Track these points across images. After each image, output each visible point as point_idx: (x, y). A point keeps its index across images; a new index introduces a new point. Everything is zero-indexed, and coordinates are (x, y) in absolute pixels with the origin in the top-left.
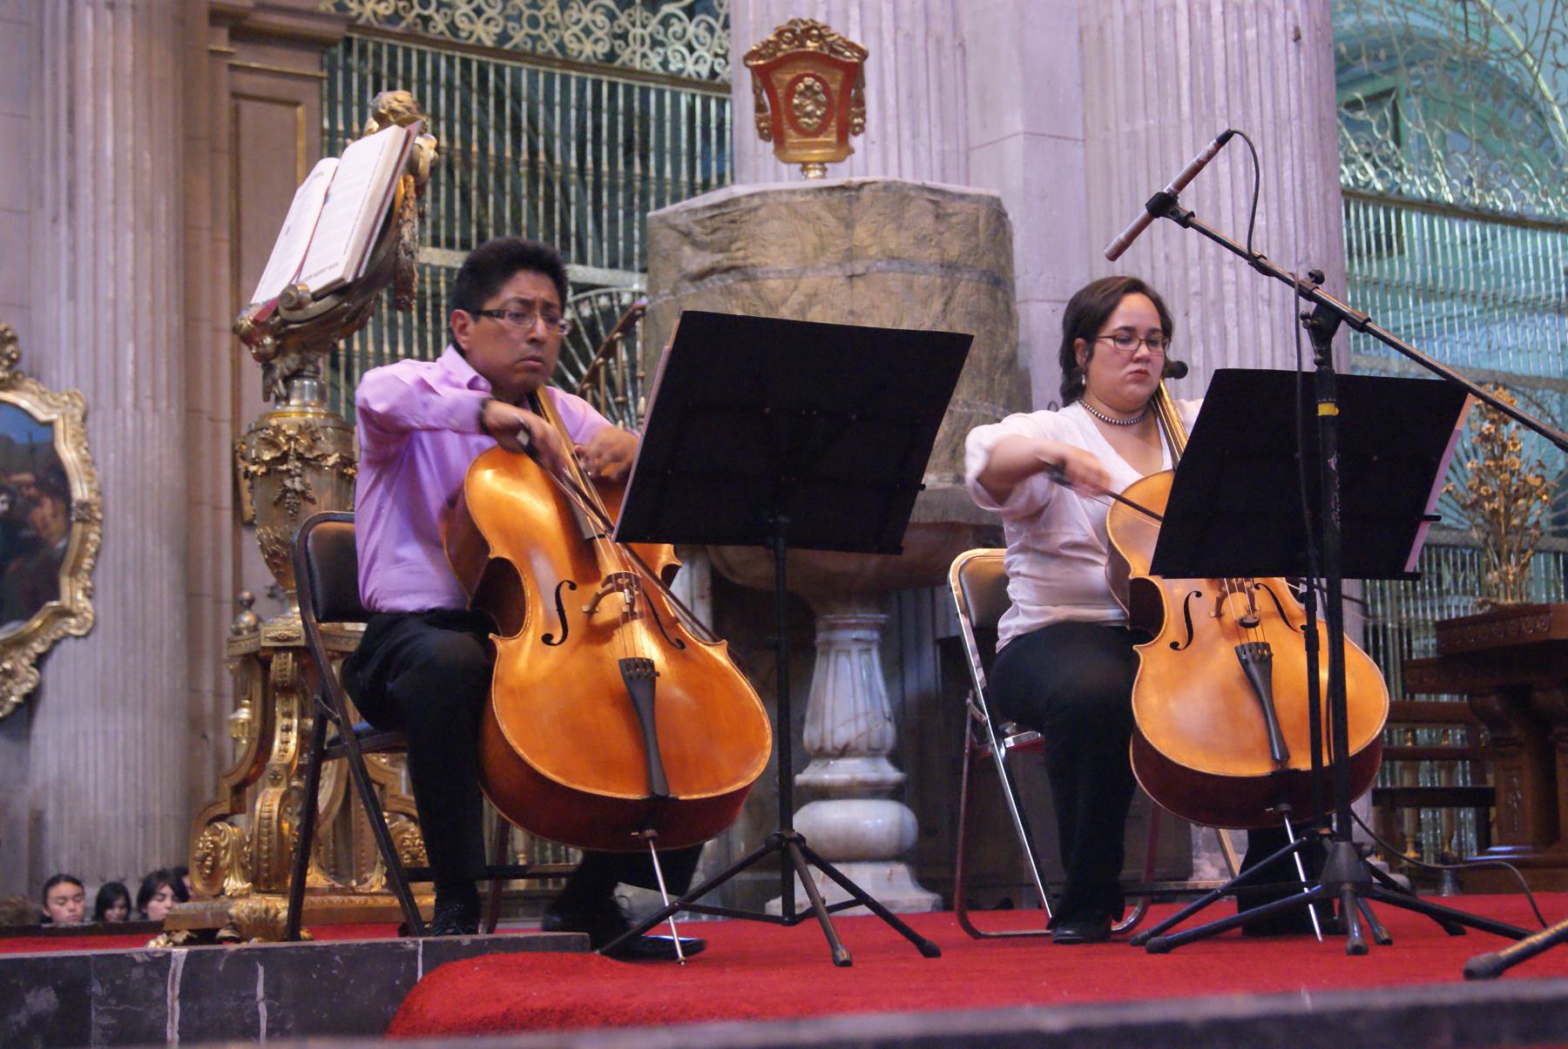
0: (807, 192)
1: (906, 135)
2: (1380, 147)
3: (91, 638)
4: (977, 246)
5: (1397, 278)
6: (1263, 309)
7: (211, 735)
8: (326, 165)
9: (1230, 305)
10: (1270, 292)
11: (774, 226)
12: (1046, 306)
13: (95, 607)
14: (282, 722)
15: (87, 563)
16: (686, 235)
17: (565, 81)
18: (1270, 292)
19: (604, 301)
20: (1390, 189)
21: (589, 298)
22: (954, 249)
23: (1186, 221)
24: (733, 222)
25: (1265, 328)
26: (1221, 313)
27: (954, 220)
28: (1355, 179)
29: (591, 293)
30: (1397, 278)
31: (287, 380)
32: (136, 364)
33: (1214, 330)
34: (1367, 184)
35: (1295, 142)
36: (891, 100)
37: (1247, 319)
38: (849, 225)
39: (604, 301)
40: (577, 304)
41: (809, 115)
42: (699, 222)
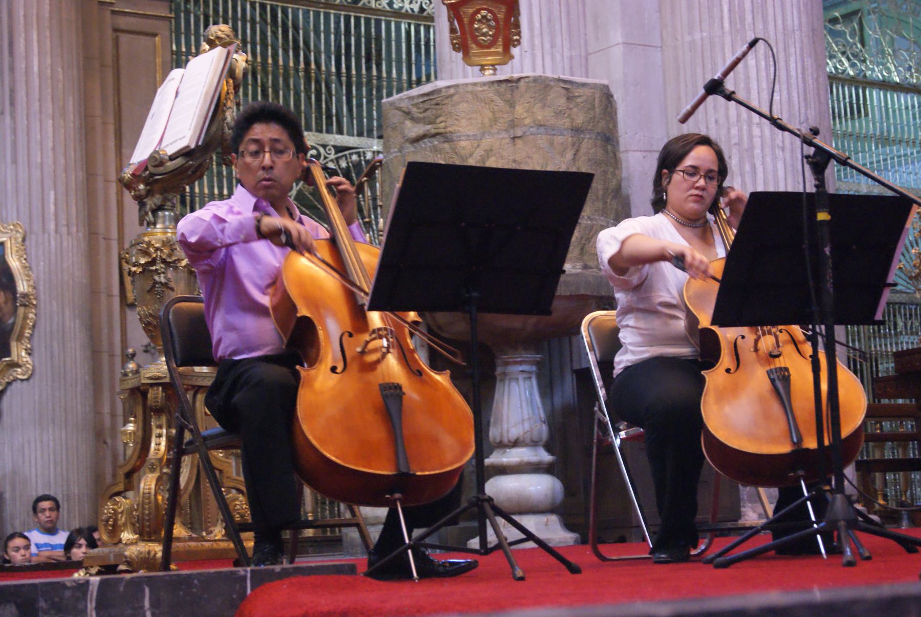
0: (484, 84)
1: (547, 46)
2: (851, 47)
3: (31, 381)
4: (594, 117)
5: (864, 132)
6: (779, 153)
7: (109, 441)
8: (176, 73)
9: (757, 151)
10: (783, 142)
11: (464, 106)
12: (639, 153)
13: (33, 361)
14: (156, 431)
15: (27, 332)
16: (407, 113)
17: (327, 16)
18: (783, 142)
19: (355, 157)
20: (858, 74)
21: (345, 156)
22: (580, 119)
23: (729, 97)
24: (438, 104)
25: (780, 165)
26: (752, 156)
27: (579, 100)
28: (836, 68)
29: (347, 153)
30: (864, 132)
31: (154, 212)
32: (56, 204)
33: (747, 167)
34: (844, 71)
35: (797, 45)
36: (537, 24)
37: (768, 159)
38: (512, 105)
39: (355, 157)
40: (337, 159)
41: (484, 35)
42: (415, 105)
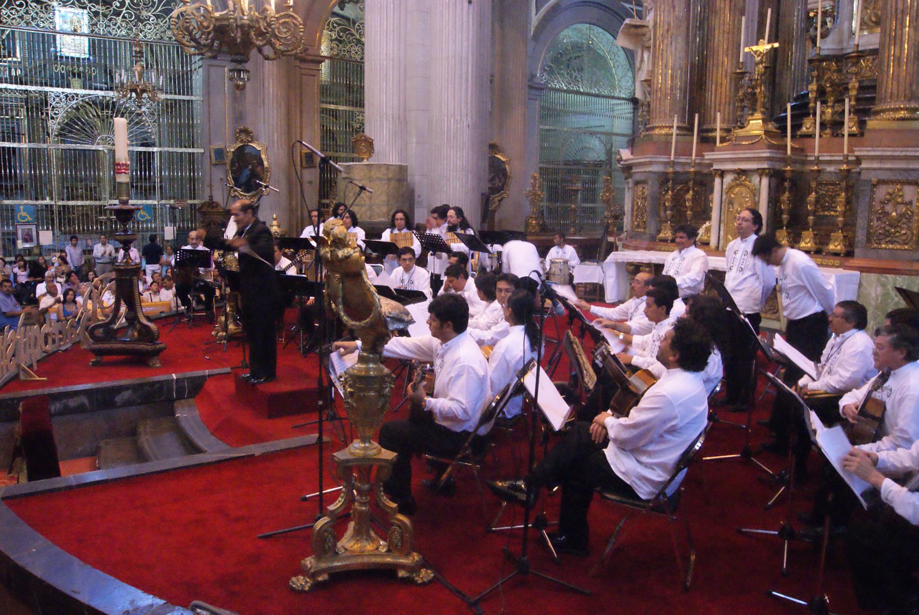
22: (391, 176)
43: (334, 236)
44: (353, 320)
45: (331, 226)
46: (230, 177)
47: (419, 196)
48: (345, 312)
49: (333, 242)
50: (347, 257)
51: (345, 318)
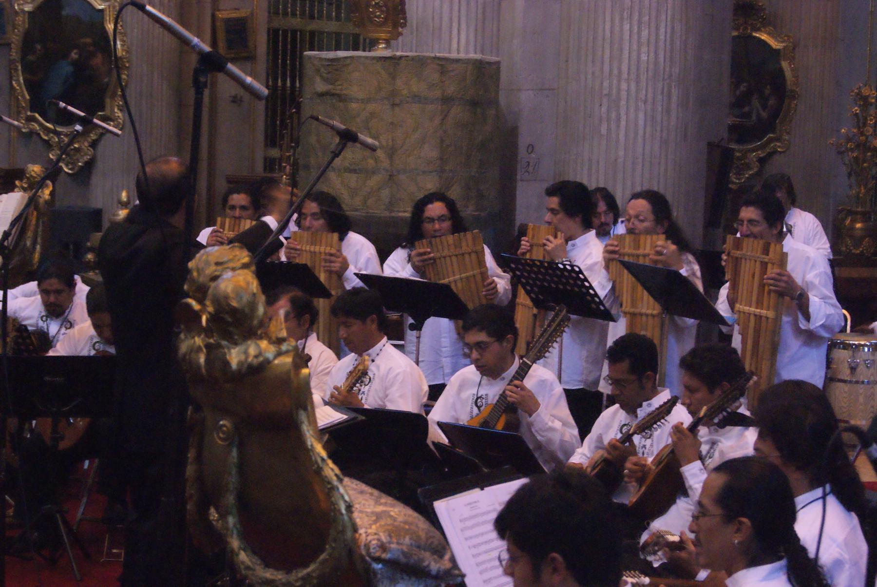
0: (373, 58)
6: (641, 105)
9: (623, 103)
11: (356, 74)
12: (531, 92)
24: (337, 70)
25: (641, 116)
26: (619, 107)
27: (452, 74)
35: (669, 13)
37: (632, 111)
38: (394, 78)
41: (379, 17)
42: (323, 65)
43: (216, 301)
44: (267, 565)
45: (210, 270)
46: (19, 82)
47: (531, 148)
48: (246, 536)
49: (214, 318)
50: (257, 371)
51: (243, 556)
